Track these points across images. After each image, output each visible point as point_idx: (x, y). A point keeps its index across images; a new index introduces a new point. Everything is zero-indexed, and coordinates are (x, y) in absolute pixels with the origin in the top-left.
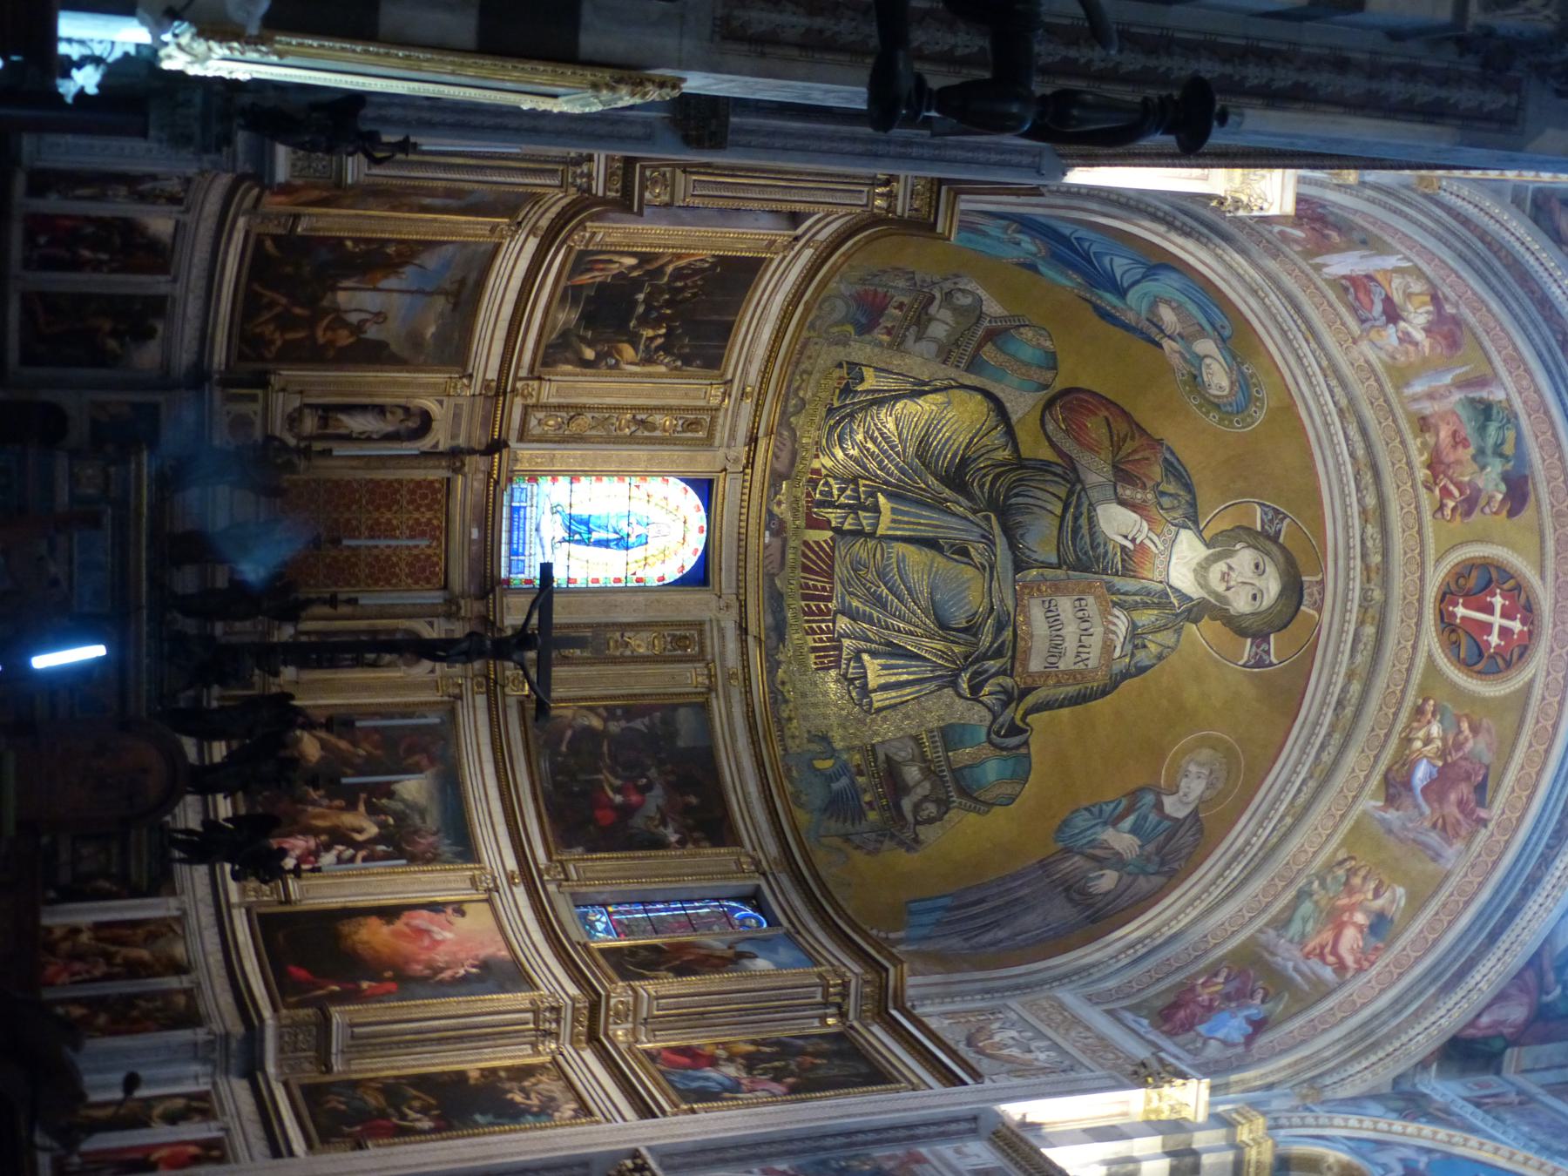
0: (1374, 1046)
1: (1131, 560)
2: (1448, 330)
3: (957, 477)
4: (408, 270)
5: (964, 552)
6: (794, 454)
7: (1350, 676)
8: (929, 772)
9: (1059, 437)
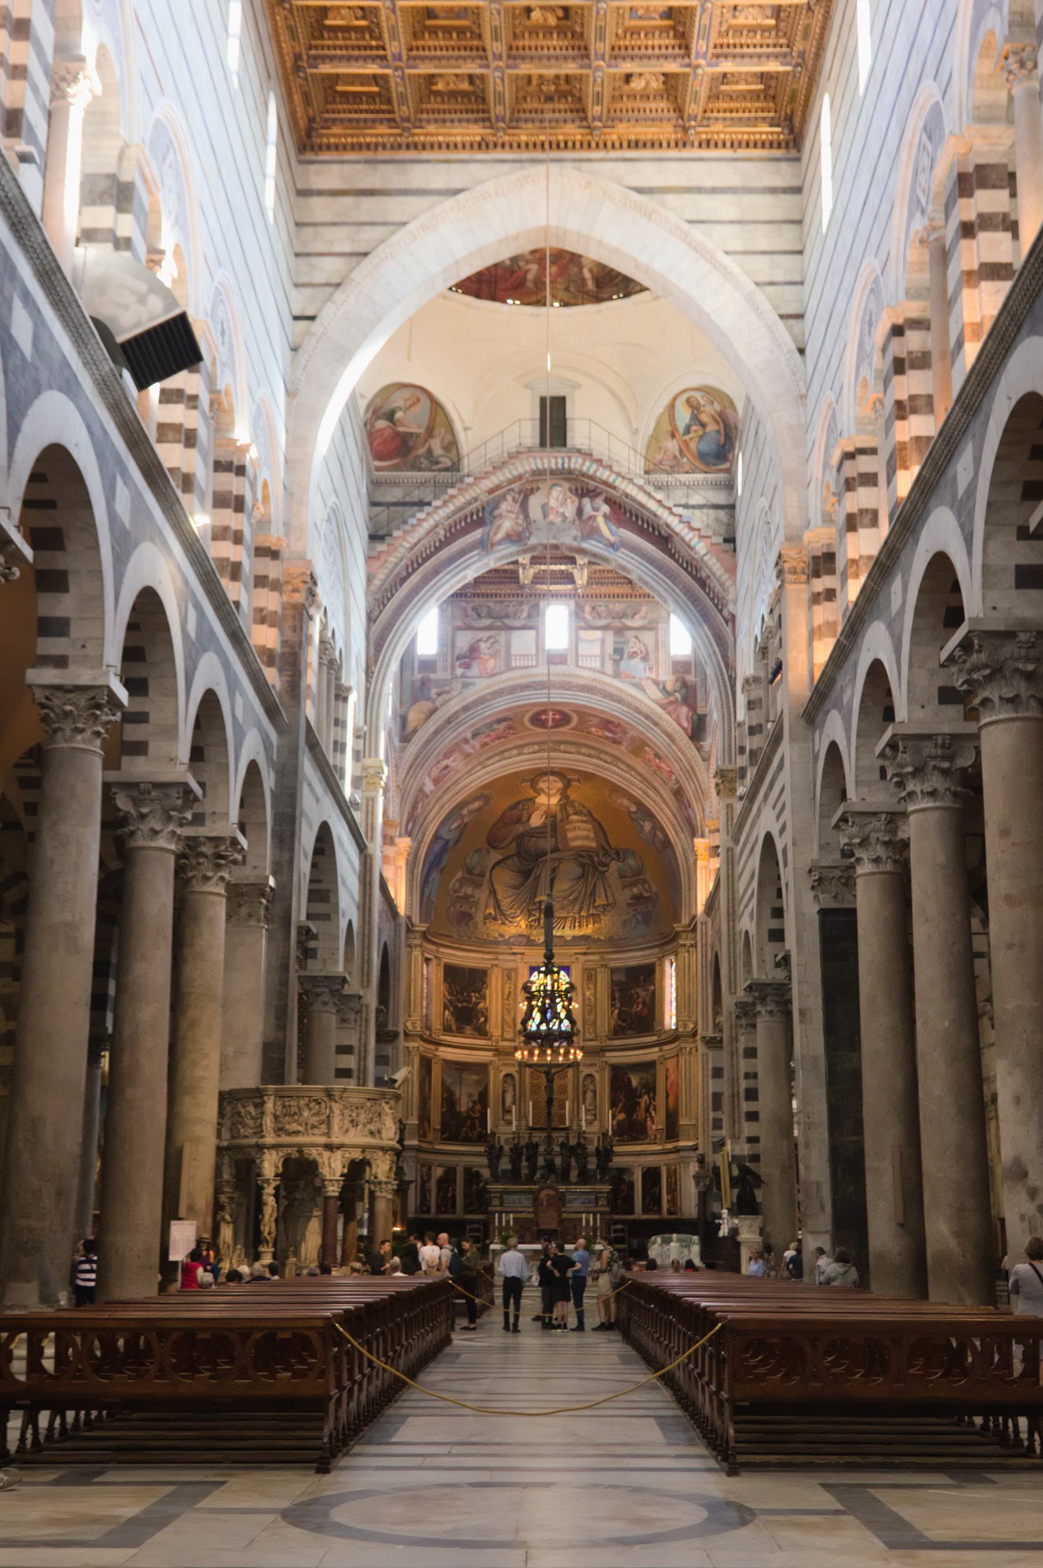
0: (692, 768)
1: (550, 815)
2: (446, 756)
3: (526, 874)
4: (453, 1088)
5: (554, 870)
6: (520, 935)
7: (579, 753)
8: (634, 884)
9: (507, 842)
